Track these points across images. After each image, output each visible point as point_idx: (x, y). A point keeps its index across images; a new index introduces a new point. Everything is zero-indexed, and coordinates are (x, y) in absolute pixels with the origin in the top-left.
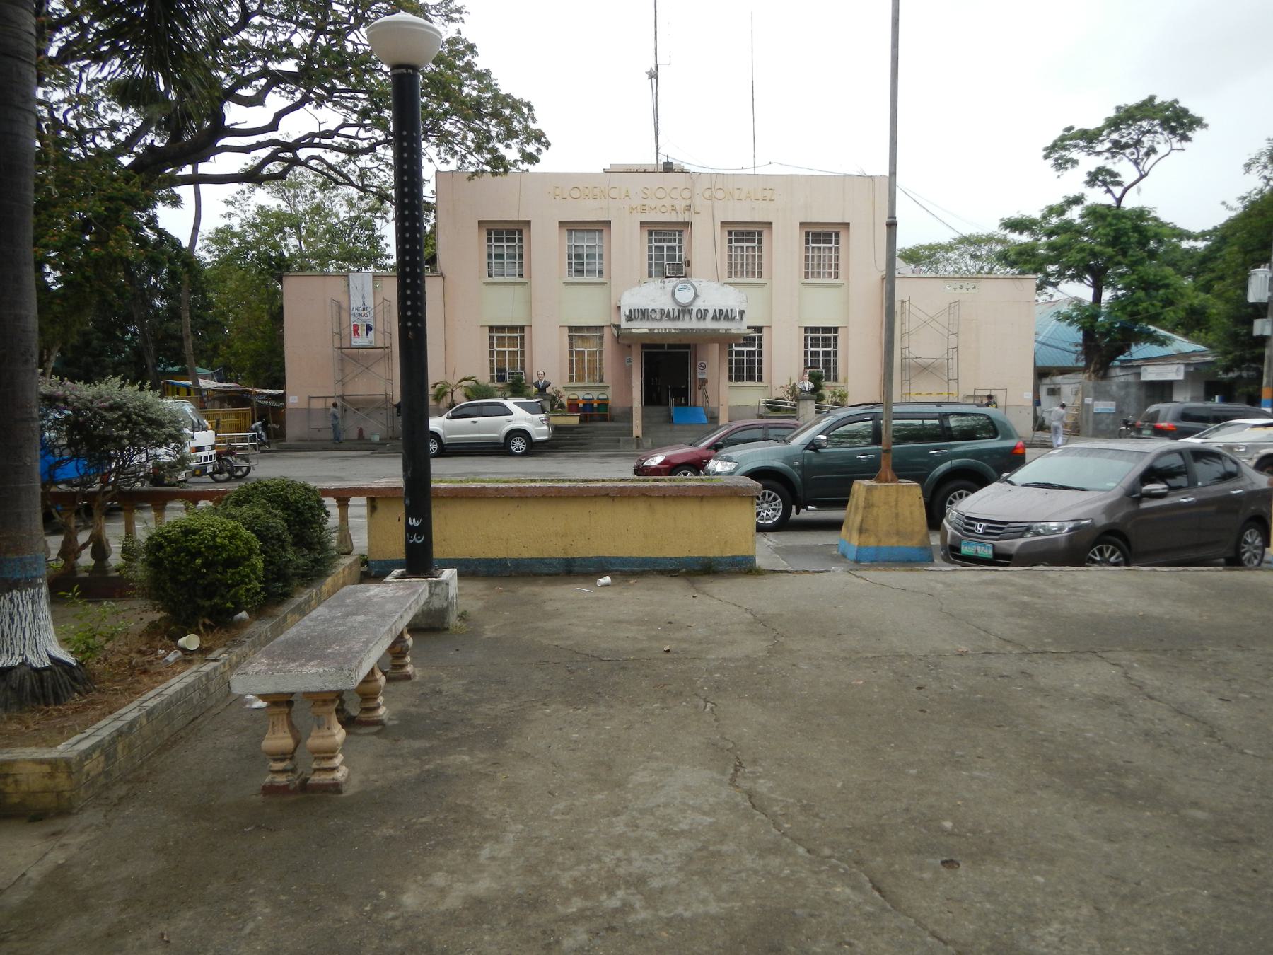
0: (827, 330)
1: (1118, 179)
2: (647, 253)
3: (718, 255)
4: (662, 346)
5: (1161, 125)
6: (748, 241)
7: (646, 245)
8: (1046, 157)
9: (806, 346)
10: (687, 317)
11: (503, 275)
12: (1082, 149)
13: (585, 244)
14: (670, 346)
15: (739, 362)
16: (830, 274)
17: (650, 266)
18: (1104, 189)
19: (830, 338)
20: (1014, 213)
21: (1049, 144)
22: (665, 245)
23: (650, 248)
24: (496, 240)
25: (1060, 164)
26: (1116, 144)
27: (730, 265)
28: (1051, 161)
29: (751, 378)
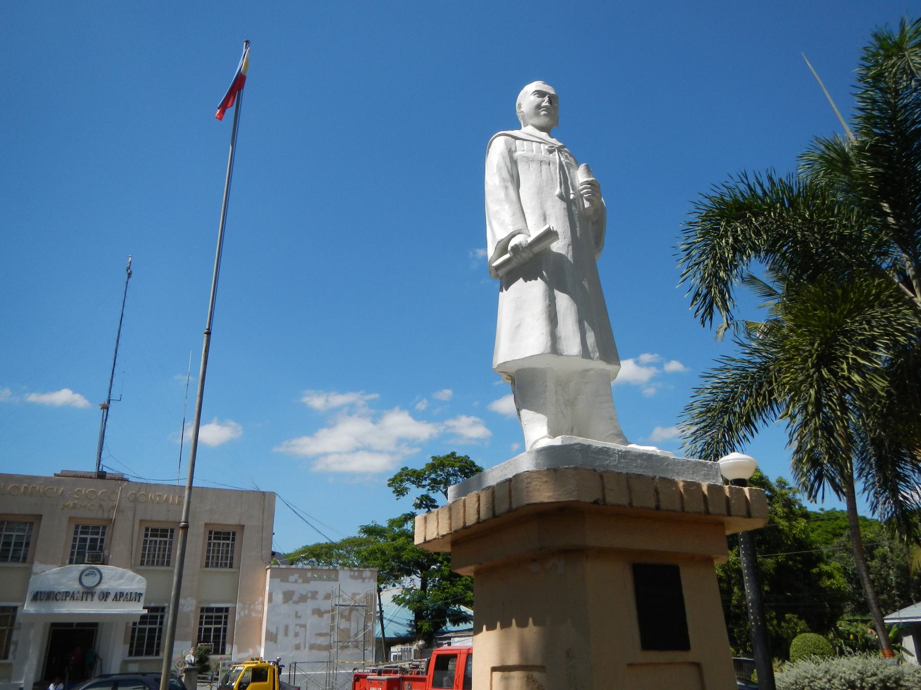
0: (219, 610)
1: (435, 504)
2: (71, 543)
3: (134, 546)
4: (71, 624)
5: (460, 470)
6: (161, 536)
7: (72, 536)
8: (390, 485)
9: (201, 623)
10: (90, 597)
12: (413, 482)
14: (79, 624)
15: (141, 639)
16: (217, 564)
17: (72, 554)
18: (427, 510)
19: (157, 617)
20: (368, 522)
21: (392, 477)
23: (75, 539)
25: (399, 491)
26: (434, 480)
27: (143, 556)
28: (392, 489)
29: (149, 653)
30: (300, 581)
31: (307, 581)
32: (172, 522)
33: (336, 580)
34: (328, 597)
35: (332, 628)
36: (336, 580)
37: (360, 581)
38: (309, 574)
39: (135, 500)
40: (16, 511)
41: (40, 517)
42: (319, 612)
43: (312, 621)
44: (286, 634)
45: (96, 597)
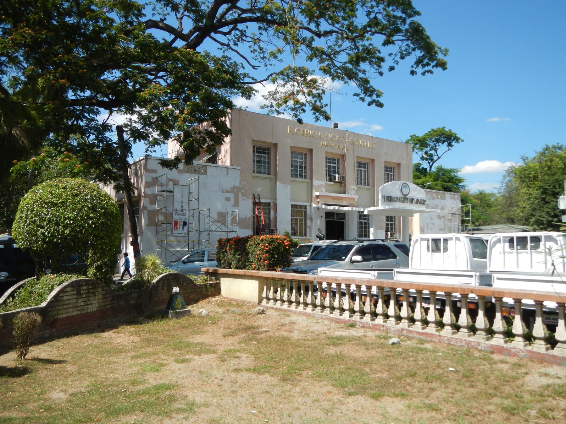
11: (260, 173)
13: (298, 160)
22: (332, 165)
24: (257, 152)
30: (431, 198)
31: (433, 199)
32: (368, 159)
33: (444, 199)
34: (442, 208)
35: (445, 227)
36: (444, 199)
37: (454, 200)
38: (434, 195)
39: (353, 144)
40: (301, 146)
41: (311, 151)
42: (439, 217)
43: (437, 221)
44: (428, 229)
45: (408, 201)
